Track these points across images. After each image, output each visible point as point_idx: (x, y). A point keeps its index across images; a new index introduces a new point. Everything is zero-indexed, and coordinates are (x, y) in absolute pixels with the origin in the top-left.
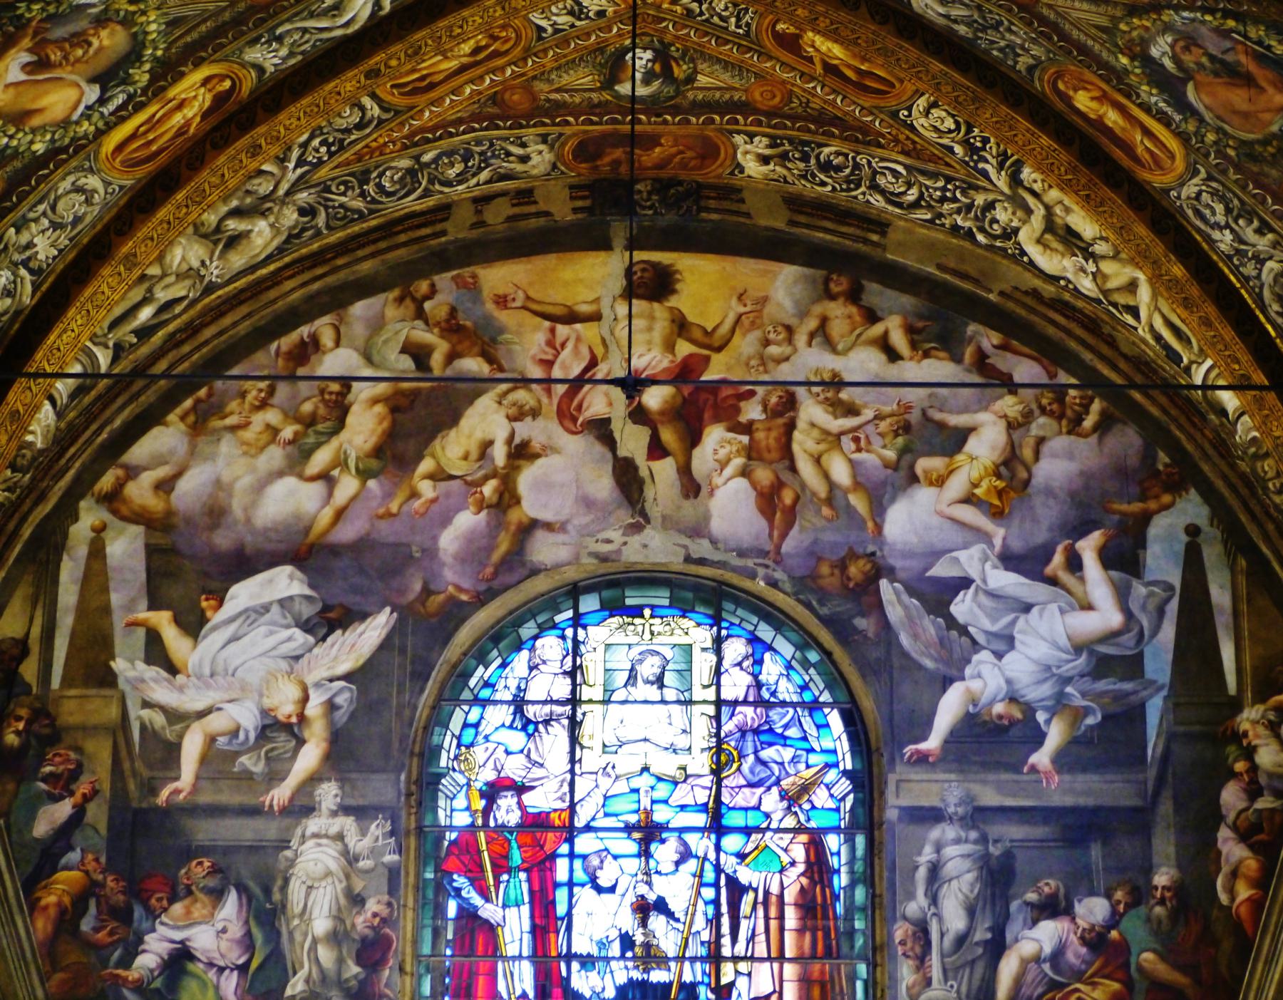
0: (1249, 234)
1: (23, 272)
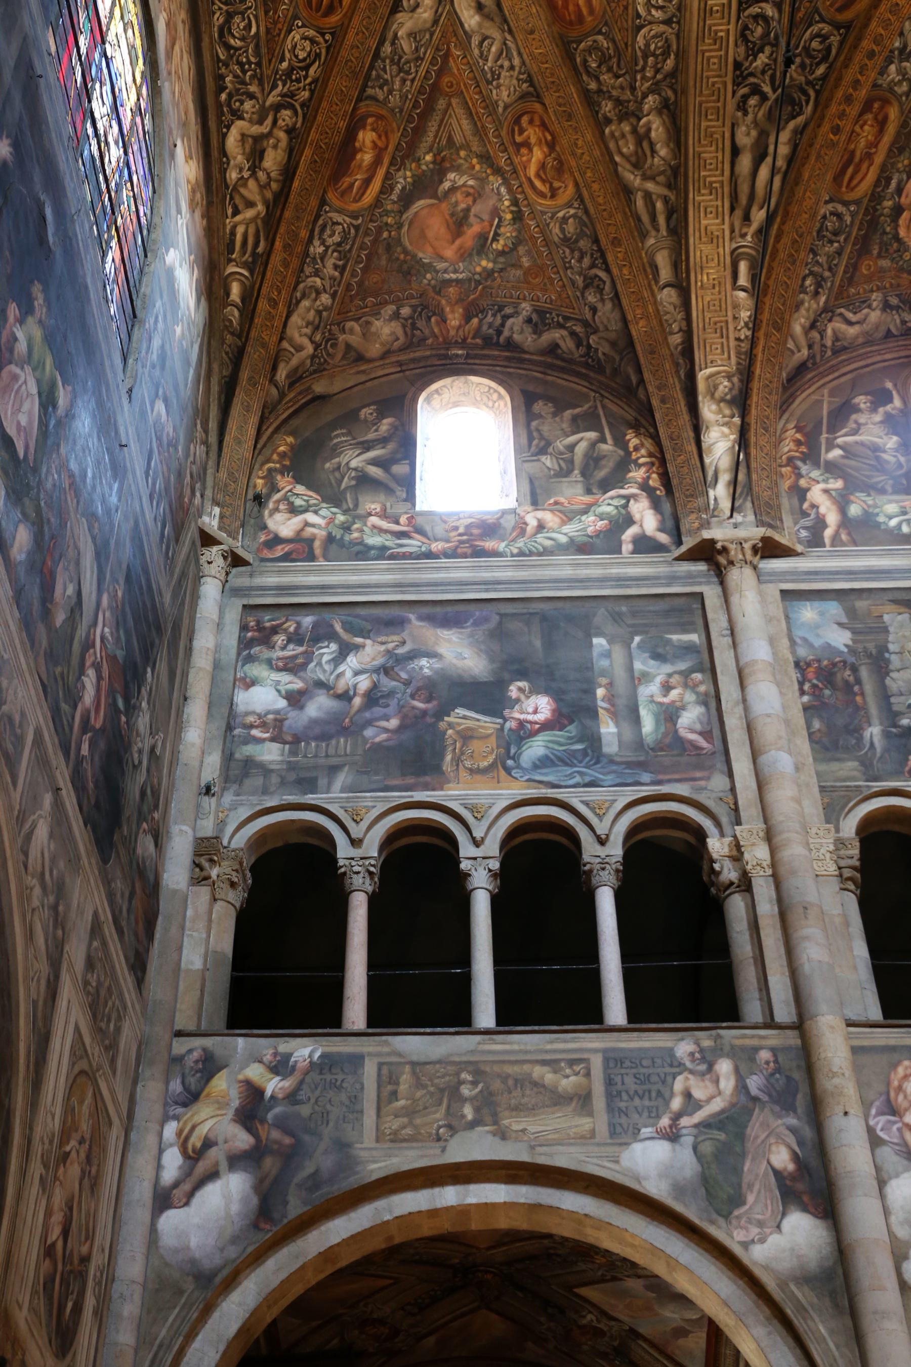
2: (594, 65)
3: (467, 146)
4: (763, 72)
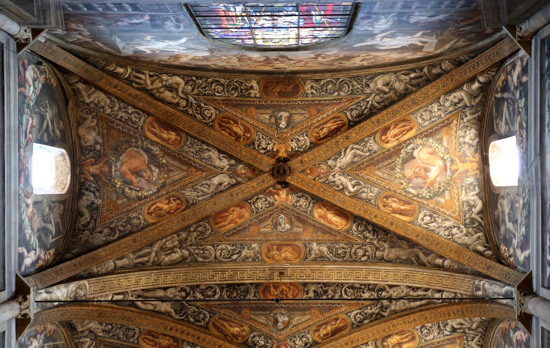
0: (124, 115)
1: (442, 103)
2: (200, 229)
3: (169, 177)
4: (194, 297)
